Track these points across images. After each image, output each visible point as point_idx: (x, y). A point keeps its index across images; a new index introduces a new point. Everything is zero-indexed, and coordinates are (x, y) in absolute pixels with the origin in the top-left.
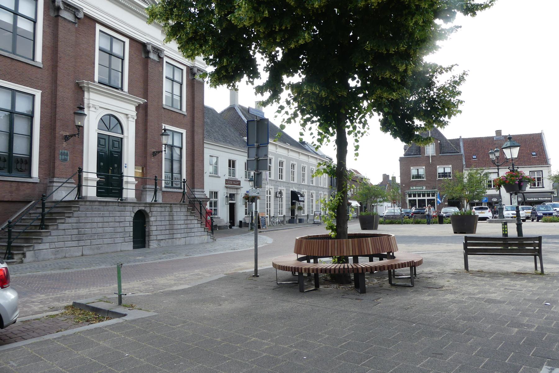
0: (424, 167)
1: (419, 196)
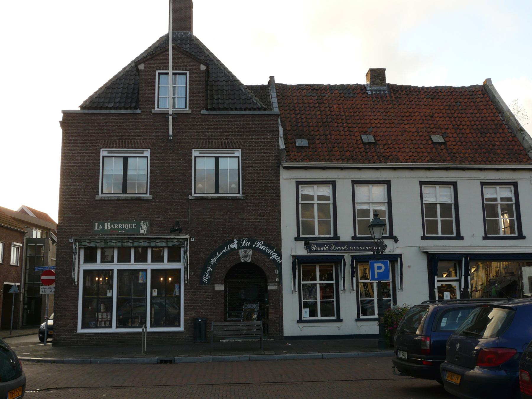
0: (147, 153)
1: (124, 258)
